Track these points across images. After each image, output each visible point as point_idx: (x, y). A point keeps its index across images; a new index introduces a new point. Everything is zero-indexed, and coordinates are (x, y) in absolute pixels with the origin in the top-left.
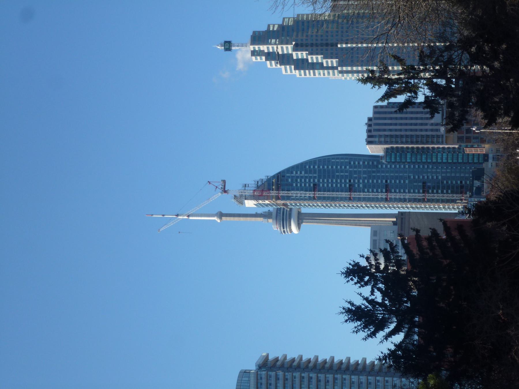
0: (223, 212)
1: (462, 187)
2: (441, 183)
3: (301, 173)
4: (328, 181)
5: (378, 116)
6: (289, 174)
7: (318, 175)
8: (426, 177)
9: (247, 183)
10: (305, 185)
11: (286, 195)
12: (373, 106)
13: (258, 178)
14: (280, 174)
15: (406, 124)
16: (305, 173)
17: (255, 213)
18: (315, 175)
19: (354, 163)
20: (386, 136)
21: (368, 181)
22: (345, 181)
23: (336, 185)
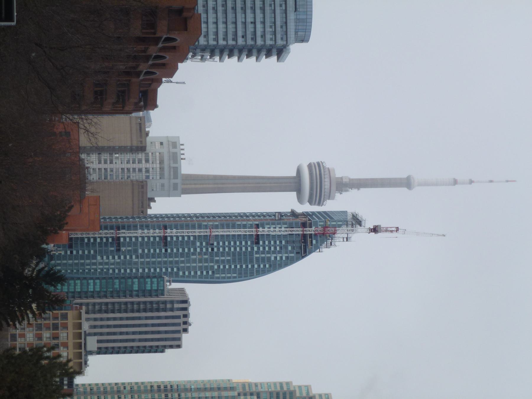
0: (405, 189)
1: (70, 246)
2: (98, 251)
3: (276, 258)
4: (241, 249)
6: (290, 257)
7: (253, 256)
8: (116, 257)
9: (346, 243)
10: (270, 242)
11: (292, 229)
12: (182, 348)
13: (332, 249)
14: (303, 255)
15: (139, 326)
16: (270, 258)
17: (361, 189)
18: (258, 256)
19: (208, 272)
20: (165, 310)
21: (189, 250)
22: (218, 249)
23: (230, 243)
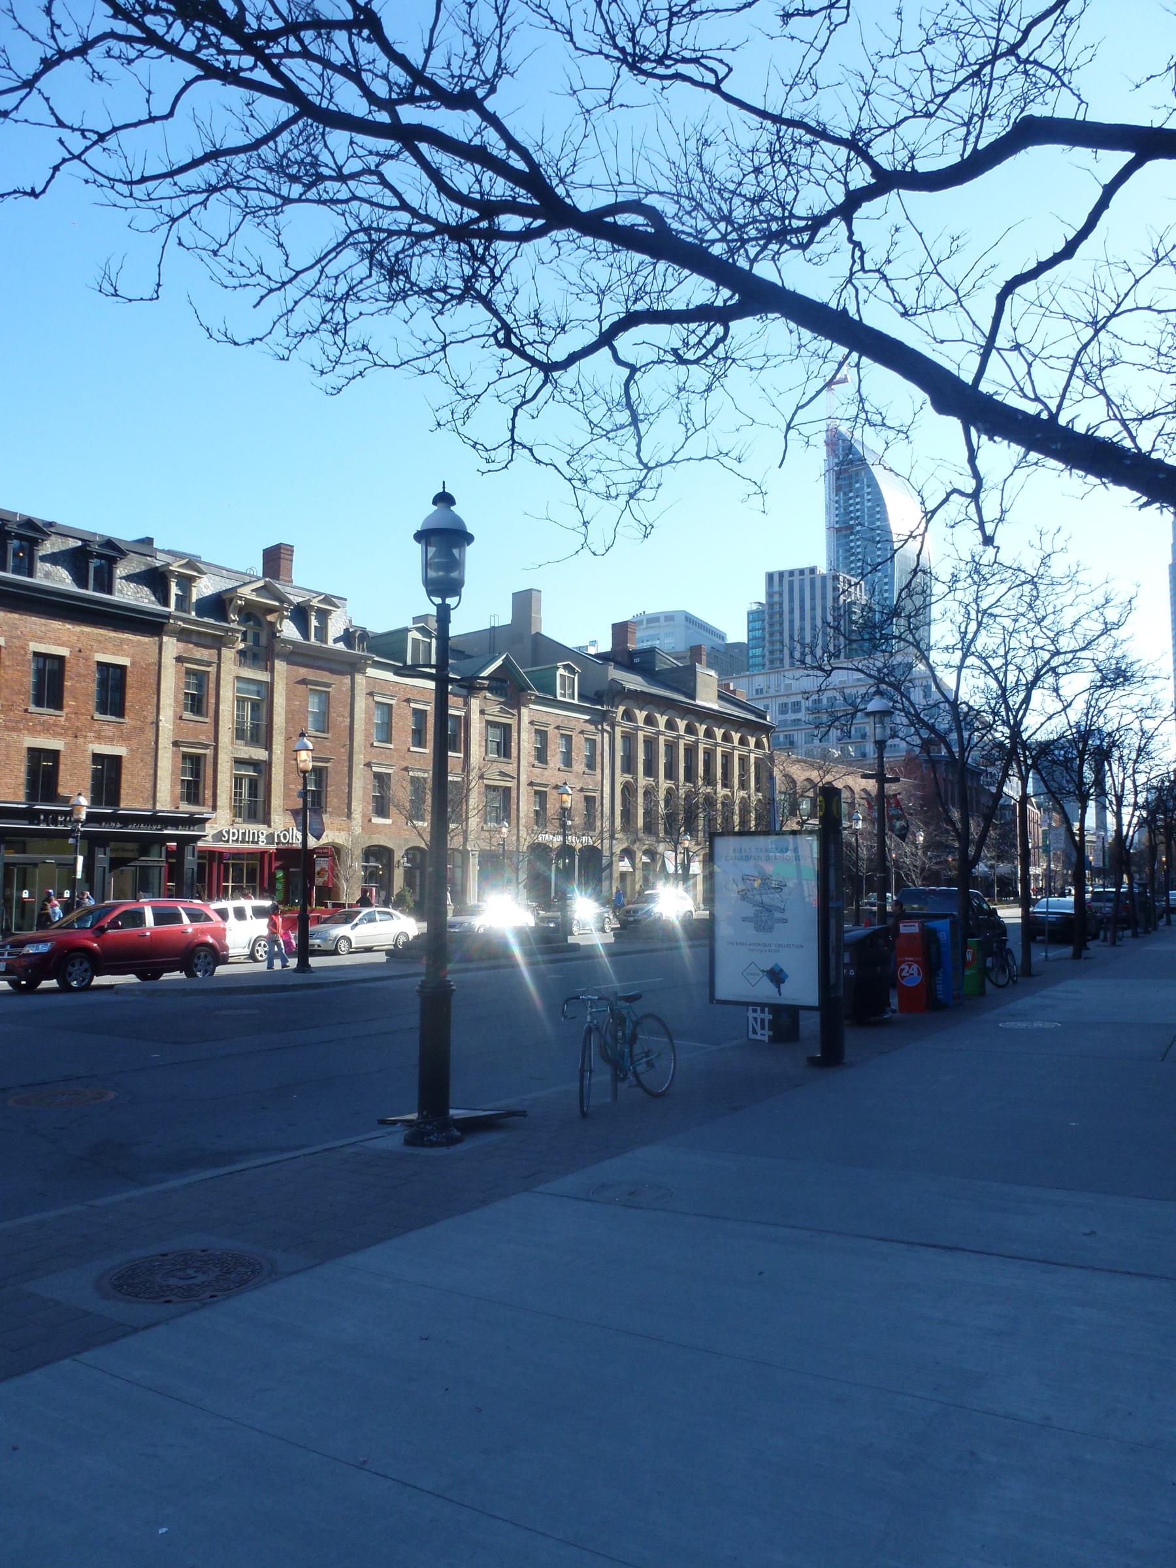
3: (869, 500)
5: (818, 583)
16: (869, 508)
20: (781, 604)
